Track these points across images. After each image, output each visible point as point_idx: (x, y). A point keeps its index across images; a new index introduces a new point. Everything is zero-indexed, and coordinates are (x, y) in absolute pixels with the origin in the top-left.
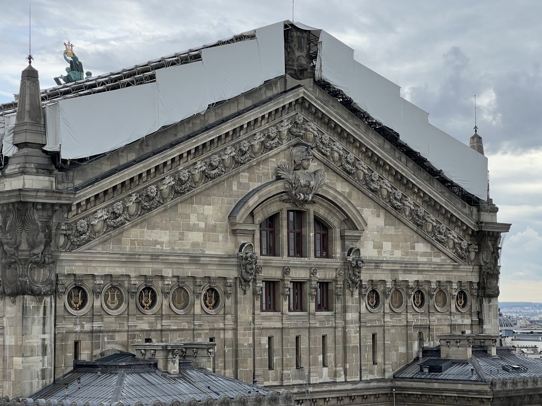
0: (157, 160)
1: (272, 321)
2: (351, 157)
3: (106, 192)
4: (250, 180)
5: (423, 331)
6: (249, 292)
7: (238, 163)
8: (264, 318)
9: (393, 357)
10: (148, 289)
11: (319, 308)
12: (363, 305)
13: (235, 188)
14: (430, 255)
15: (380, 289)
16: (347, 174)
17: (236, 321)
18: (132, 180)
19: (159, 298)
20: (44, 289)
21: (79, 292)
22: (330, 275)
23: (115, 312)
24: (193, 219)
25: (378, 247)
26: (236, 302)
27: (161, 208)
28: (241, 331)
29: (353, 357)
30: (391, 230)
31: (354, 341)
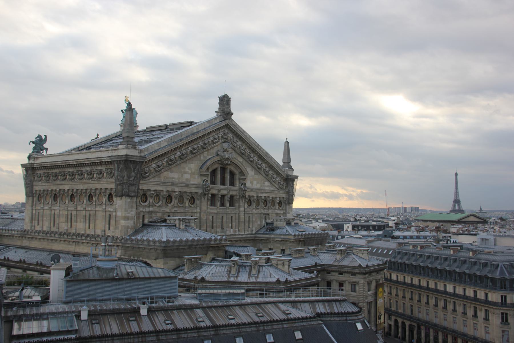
0: (175, 146)
2: (244, 147)
3: (156, 157)
4: (208, 155)
5: (266, 216)
6: (206, 199)
7: (204, 148)
8: (210, 209)
9: (256, 225)
10: (170, 196)
11: (230, 206)
12: (246, 205)
13: (202, 158)
15: (252, 199)
16: (242, 155)
17: (201, 210)
18: (165, 153)
19: (173, 200)
20: (133, 194)
21: (144, 197)
22: (234, 193)
23: (158, 205)
24: (187, 169)
25: (252, 183)
26: (201, 202)
27: (175, 165)
28: (202, 213)
29: (242, 225)
30: (256, 177)
31: (242, 219)
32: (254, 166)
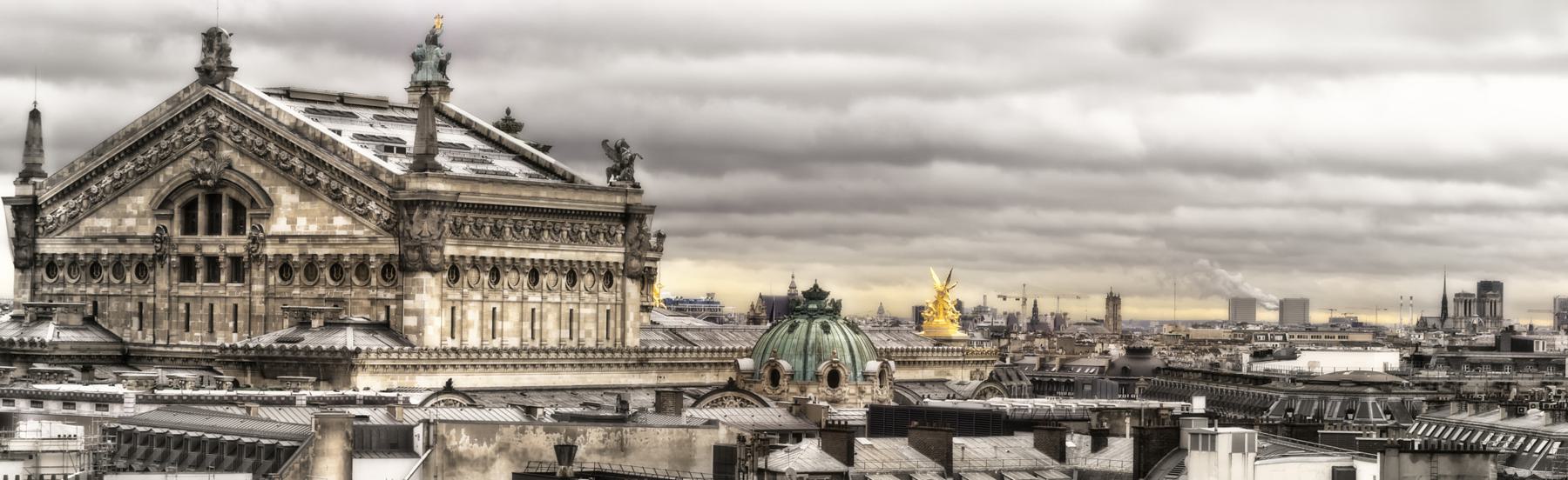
1: (190, 290)
12: (274, 278)
14: (351, 227)
21: (52, 266)
24: (129, 208)
25: (292, 222)
30: (307, 206)
32: (295, 179)
